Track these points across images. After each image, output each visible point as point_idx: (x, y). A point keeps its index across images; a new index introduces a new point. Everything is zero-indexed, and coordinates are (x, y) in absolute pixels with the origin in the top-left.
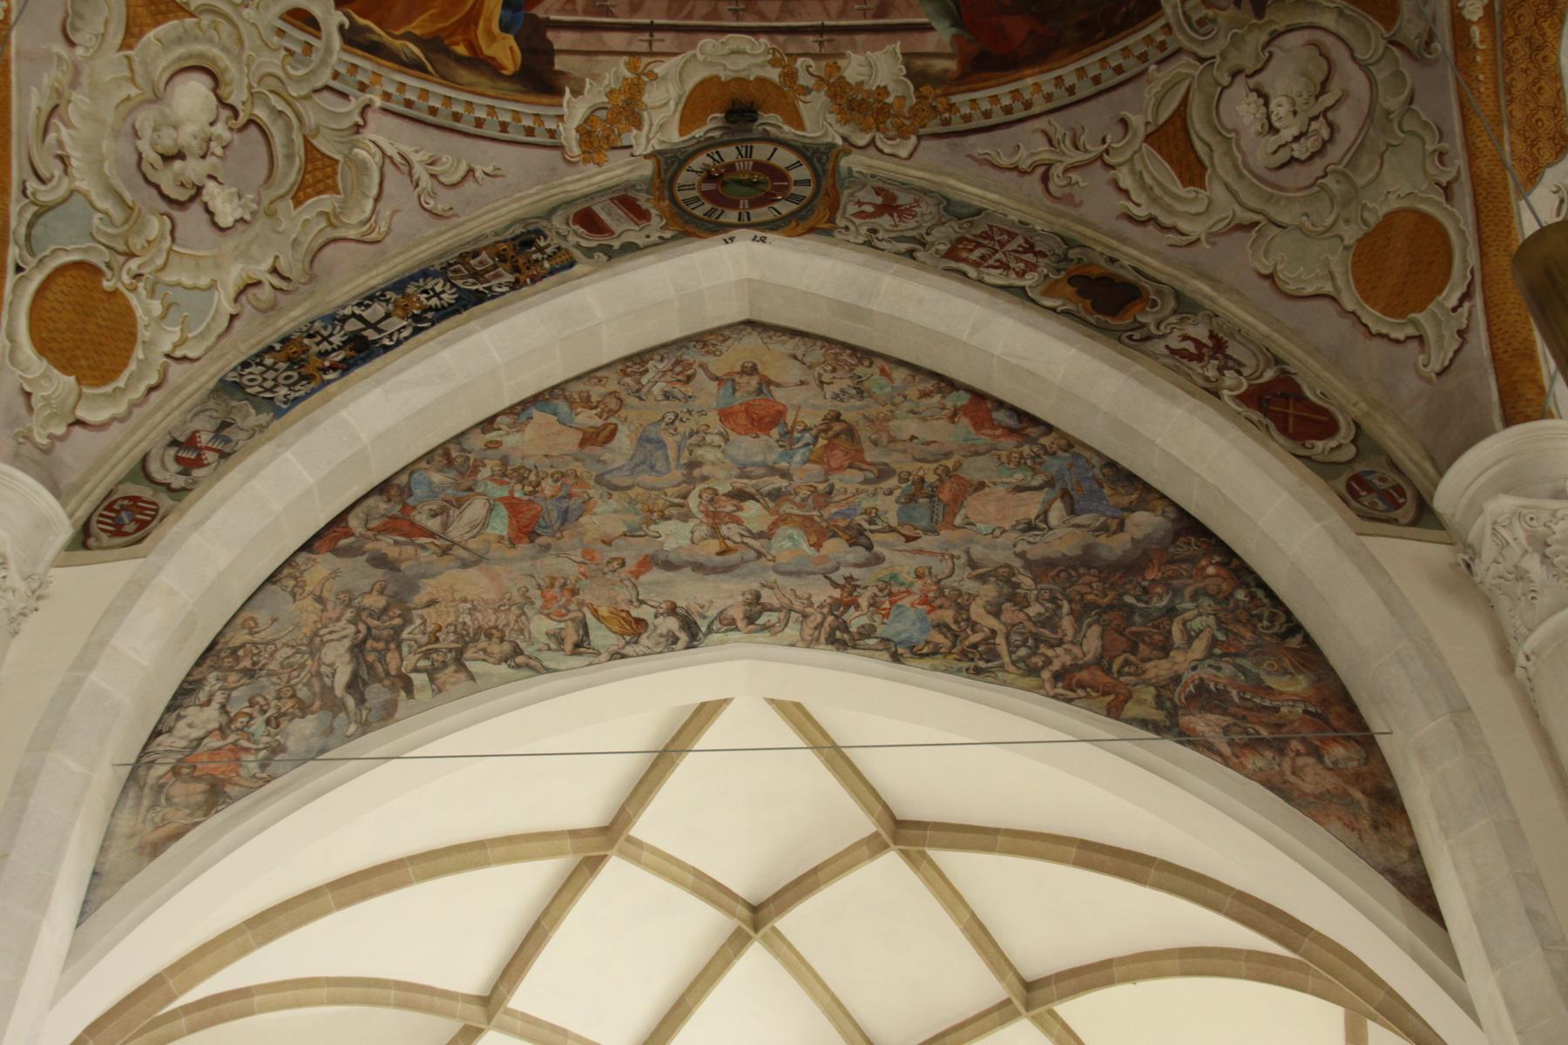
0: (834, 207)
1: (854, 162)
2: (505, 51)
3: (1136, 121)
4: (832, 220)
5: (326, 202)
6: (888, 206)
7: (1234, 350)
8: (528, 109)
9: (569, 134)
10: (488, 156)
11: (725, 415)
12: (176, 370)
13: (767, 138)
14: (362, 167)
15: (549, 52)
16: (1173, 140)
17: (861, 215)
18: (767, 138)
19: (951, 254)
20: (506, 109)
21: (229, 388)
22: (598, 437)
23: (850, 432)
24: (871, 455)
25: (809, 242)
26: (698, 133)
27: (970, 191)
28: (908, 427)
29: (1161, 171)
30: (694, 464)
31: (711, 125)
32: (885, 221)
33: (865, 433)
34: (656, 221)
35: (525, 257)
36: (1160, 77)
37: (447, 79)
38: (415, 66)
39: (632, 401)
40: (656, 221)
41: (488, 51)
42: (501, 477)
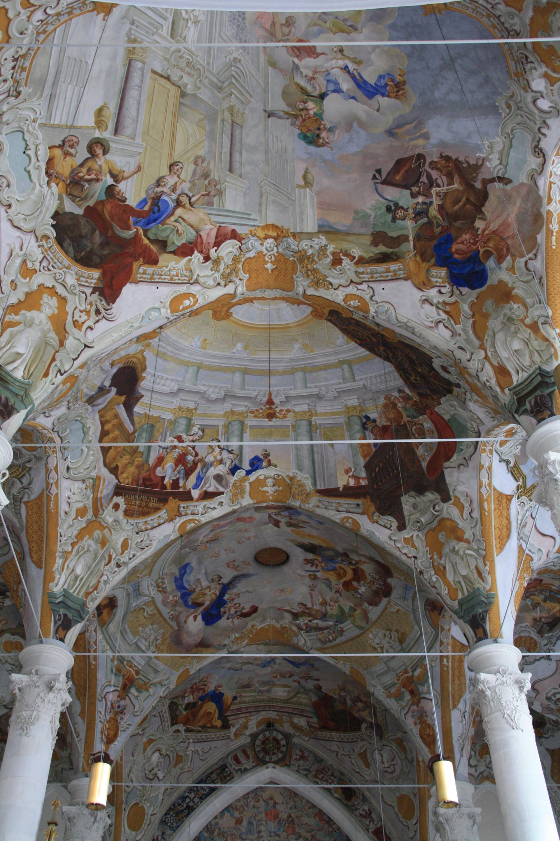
0: (291, 756)
1: (295, 740)
2: (219, 723)
3: (356, 750)
4: (290, 762)
5: (181, 765)
6: (302, 757)
7: (373, 816)
8: (223, 733)
9: (232, 735)
10: (213, 744)
11: (266, 815)
12: (153, 817)
13: (276, 730)
14: (188, 755)
15: (228, 721)
16: (363, 756)
17: (296, 759)
18: (276, 730)
19: (315, 776)
20: (218, 734)
21: (163, 822)
22: (239, 821)
23: (293, 821)
24: (297, 830)
25: (284, 769)
26: (260, 728)
27: (321, 754)
28: (305, 820)
29: (361, 762)
30: (260, 832)
31: (263, 726)
32: (302, 762)
33: (296, 821)
34: (251, 760)
35: (222, 774)
36: (361, 743)
37: (206, 732)
38: (199, 731)
39: (246, 808)
40: (251, 760)
41: (215, 724)
42: (219, 834)
